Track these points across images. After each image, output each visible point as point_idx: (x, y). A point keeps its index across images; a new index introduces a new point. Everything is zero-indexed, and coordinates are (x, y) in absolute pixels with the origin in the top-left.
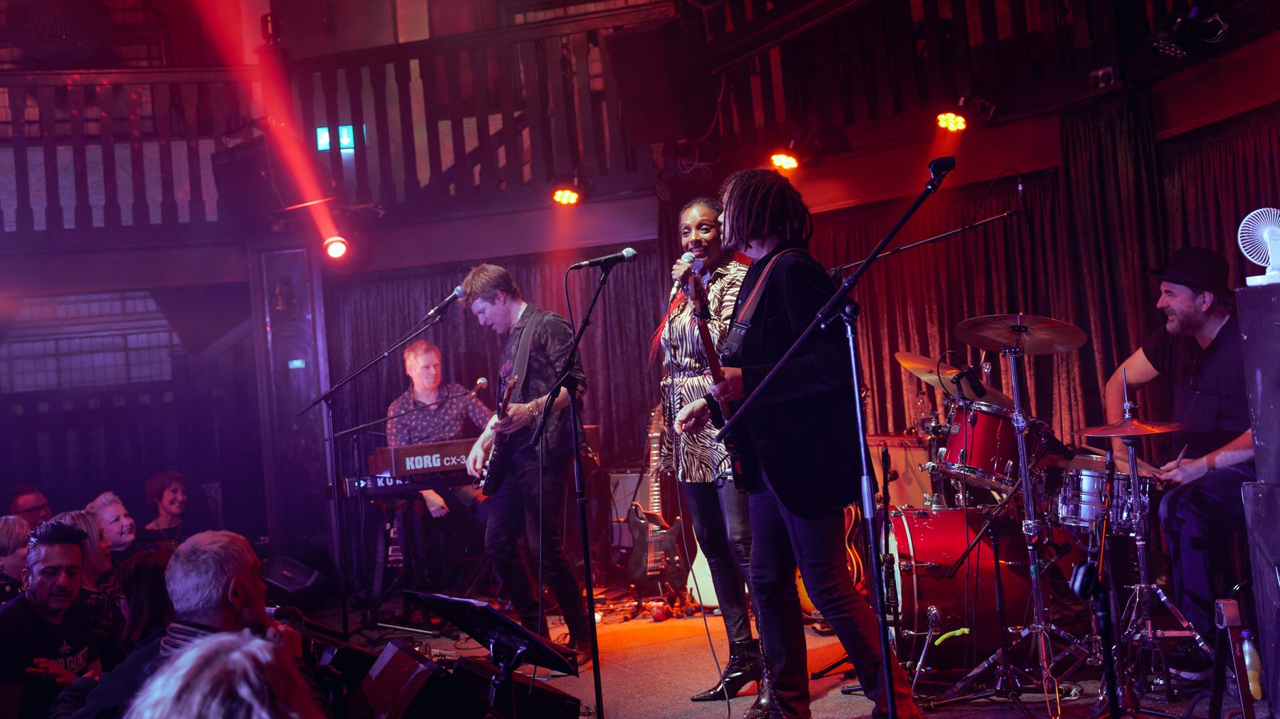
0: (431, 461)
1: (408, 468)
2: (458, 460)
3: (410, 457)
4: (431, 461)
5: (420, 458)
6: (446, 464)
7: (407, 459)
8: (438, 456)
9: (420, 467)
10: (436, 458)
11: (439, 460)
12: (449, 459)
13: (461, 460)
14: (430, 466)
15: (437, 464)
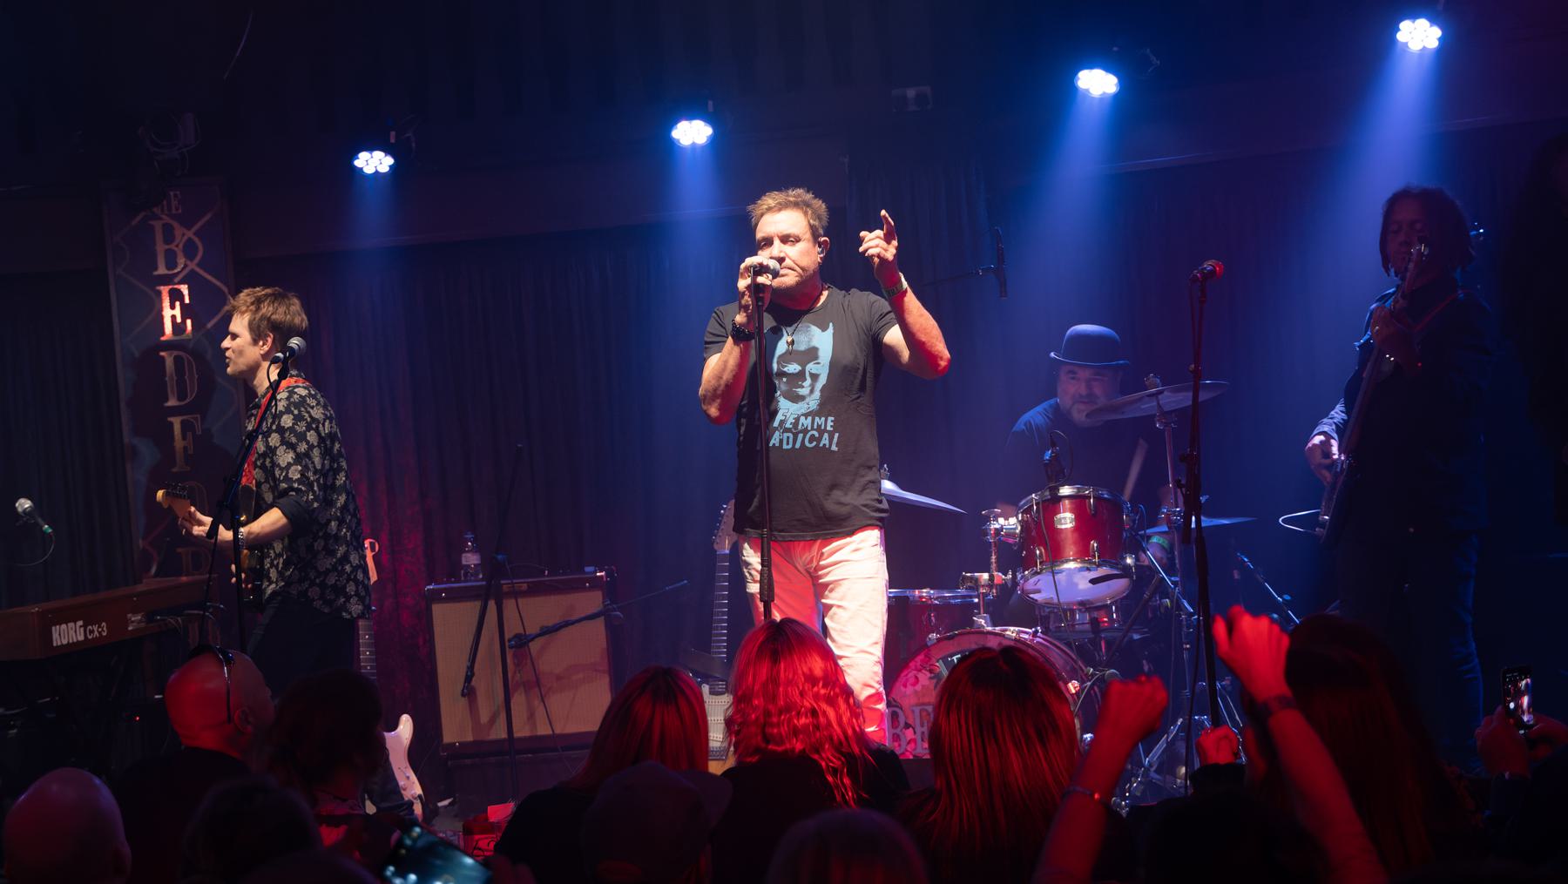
0: (76, 632)
1: (55, 644)
2: (100, 630)
3: (55, 625)
4: (76, 632)
5: (64, 626)
6: (90, 637)
7: (53, 628)
8: (80, 623)
9: (65, 642)
10: (81, 626)
11: (82, 629)
12: (90, 627)
13: (103, 630)
14: (75, 640)
15: (81, 638)
